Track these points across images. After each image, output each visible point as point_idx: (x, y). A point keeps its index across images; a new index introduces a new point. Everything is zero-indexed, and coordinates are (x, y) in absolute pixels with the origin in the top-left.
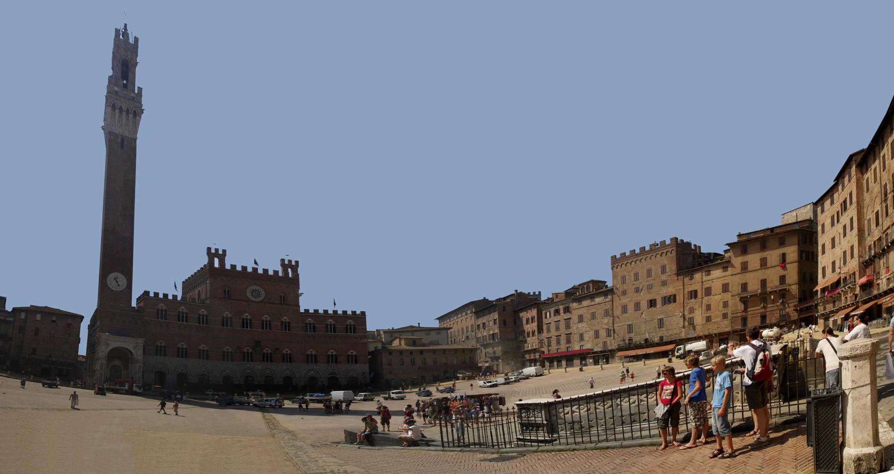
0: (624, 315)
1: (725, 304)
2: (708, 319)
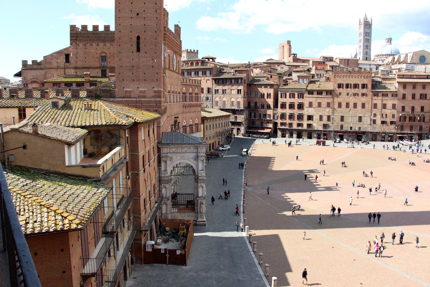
0: (339, 109)
1: (393, 116)
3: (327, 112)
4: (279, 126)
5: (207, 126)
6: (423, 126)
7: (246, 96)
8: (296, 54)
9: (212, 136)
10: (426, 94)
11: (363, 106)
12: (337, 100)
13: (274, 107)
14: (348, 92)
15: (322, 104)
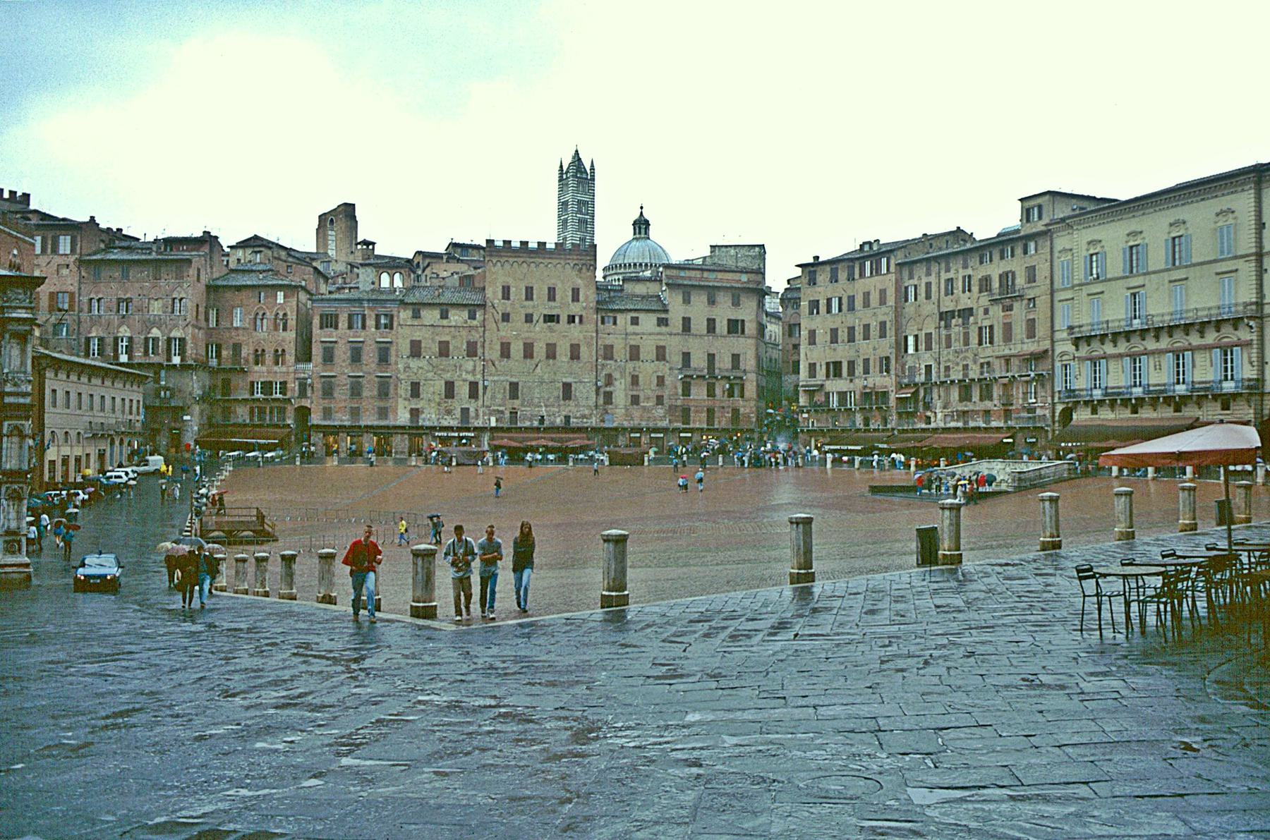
1: (661, 381)
2: (635, 400)
3: (465, 371)
4: (316, 419)
5: (54, 391)
6: (742, 410)
7: (203, 324)
8: (373, 244)
9: (73, 434)
10: (743, 321)
11: (575, 354)
12: (497, 334)
13: (298, 360)
14: (530, 311)
15: (451, 348)
